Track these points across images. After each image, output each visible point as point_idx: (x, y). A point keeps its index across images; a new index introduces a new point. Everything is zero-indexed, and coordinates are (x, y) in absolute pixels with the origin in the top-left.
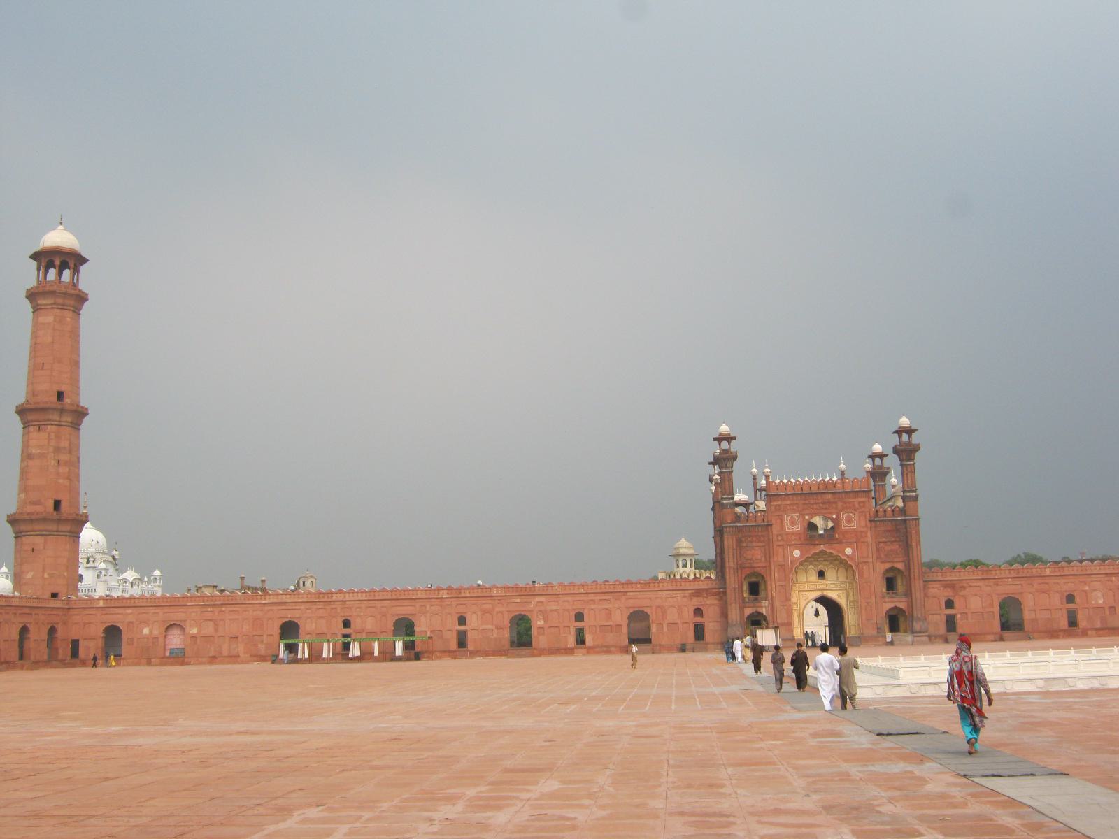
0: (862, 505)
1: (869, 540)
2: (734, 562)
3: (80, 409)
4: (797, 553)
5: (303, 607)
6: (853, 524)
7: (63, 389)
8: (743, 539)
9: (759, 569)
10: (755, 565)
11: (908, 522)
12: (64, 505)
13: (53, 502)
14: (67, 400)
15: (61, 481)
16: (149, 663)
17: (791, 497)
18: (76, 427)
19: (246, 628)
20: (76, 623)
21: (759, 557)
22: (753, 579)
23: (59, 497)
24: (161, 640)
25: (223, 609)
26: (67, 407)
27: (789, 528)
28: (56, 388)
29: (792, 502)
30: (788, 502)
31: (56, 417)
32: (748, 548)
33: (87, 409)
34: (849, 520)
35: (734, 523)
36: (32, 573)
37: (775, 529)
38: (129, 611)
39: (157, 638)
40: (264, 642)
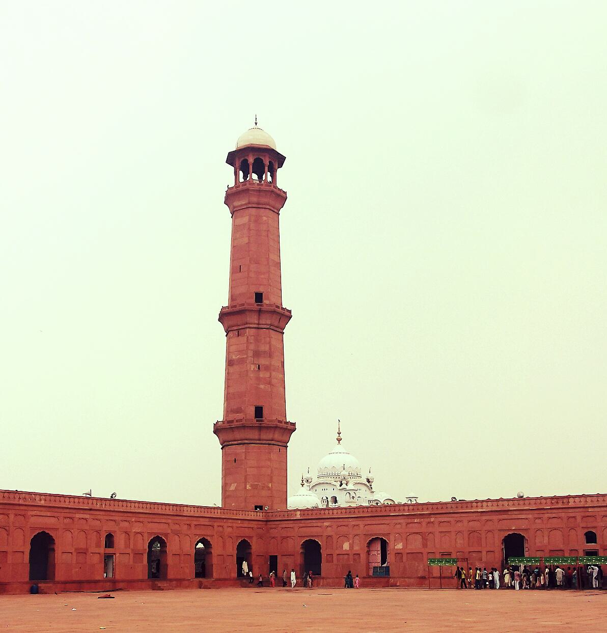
3: (280, 310)
5: (530, 516)
7: (261, 290)
12: (265, 412)
13: (253, 409)
14: (266, 302)
15: (262, 386)
16: (350, 585)
18: (280, 330)
19: (461, 542)
20: (274, 538)
23: (260, 404)
24: (363, 556)
25: (432, 520)
26: (264, 308)
28: (254, 289)
31: (253, 319)
33: (290, 312)
36: (236, 484)
38: (326, 524)
39: (359, 554)
40: (483, 560)
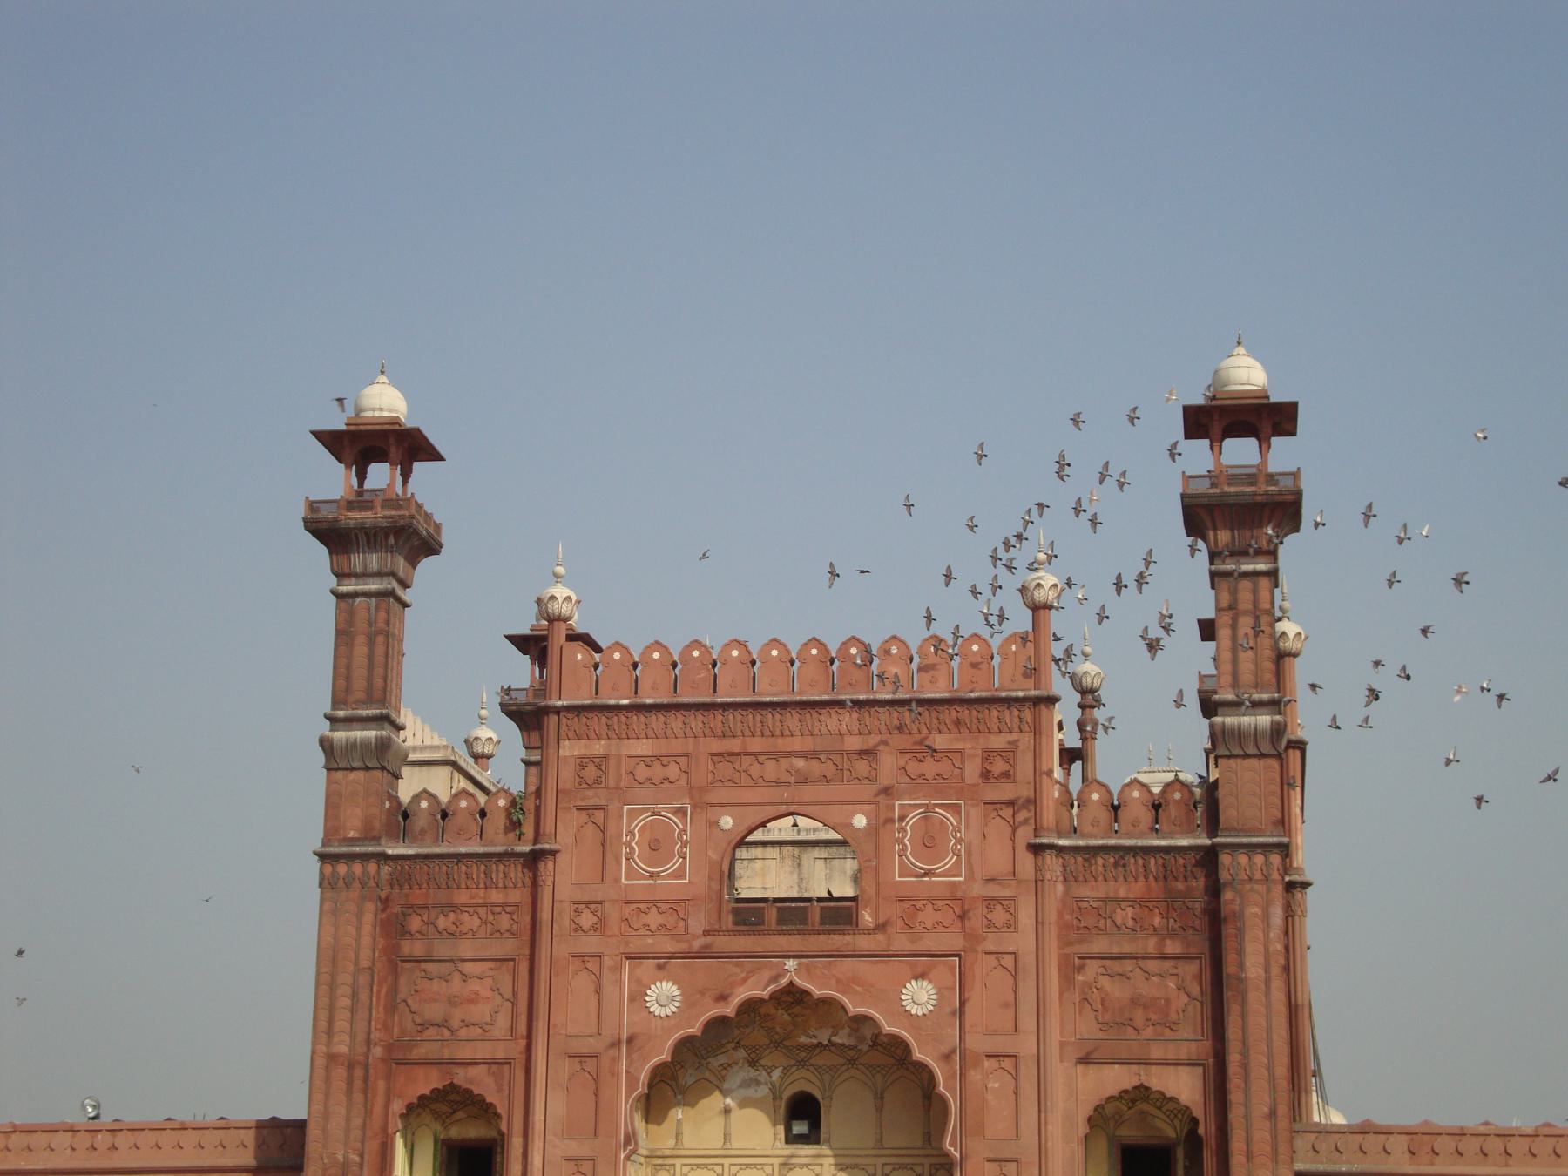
0: (999, 767)
1: (1024, 941)
2: (353, 1036)
4: (664, 996)
6: (951, 860)
8: (415, 923)
9: (473, 1072)
10: (465, 1053)
11: (1225, 858)
17: (657, 721)
21: (480, 1012)
22: (470, 1131)
27: (634, 872)
29: (662, 746)
30: (643, 747)
32: (431, 967)
34: (930, 842)
35: (376, 840)
37: (566, 878)
